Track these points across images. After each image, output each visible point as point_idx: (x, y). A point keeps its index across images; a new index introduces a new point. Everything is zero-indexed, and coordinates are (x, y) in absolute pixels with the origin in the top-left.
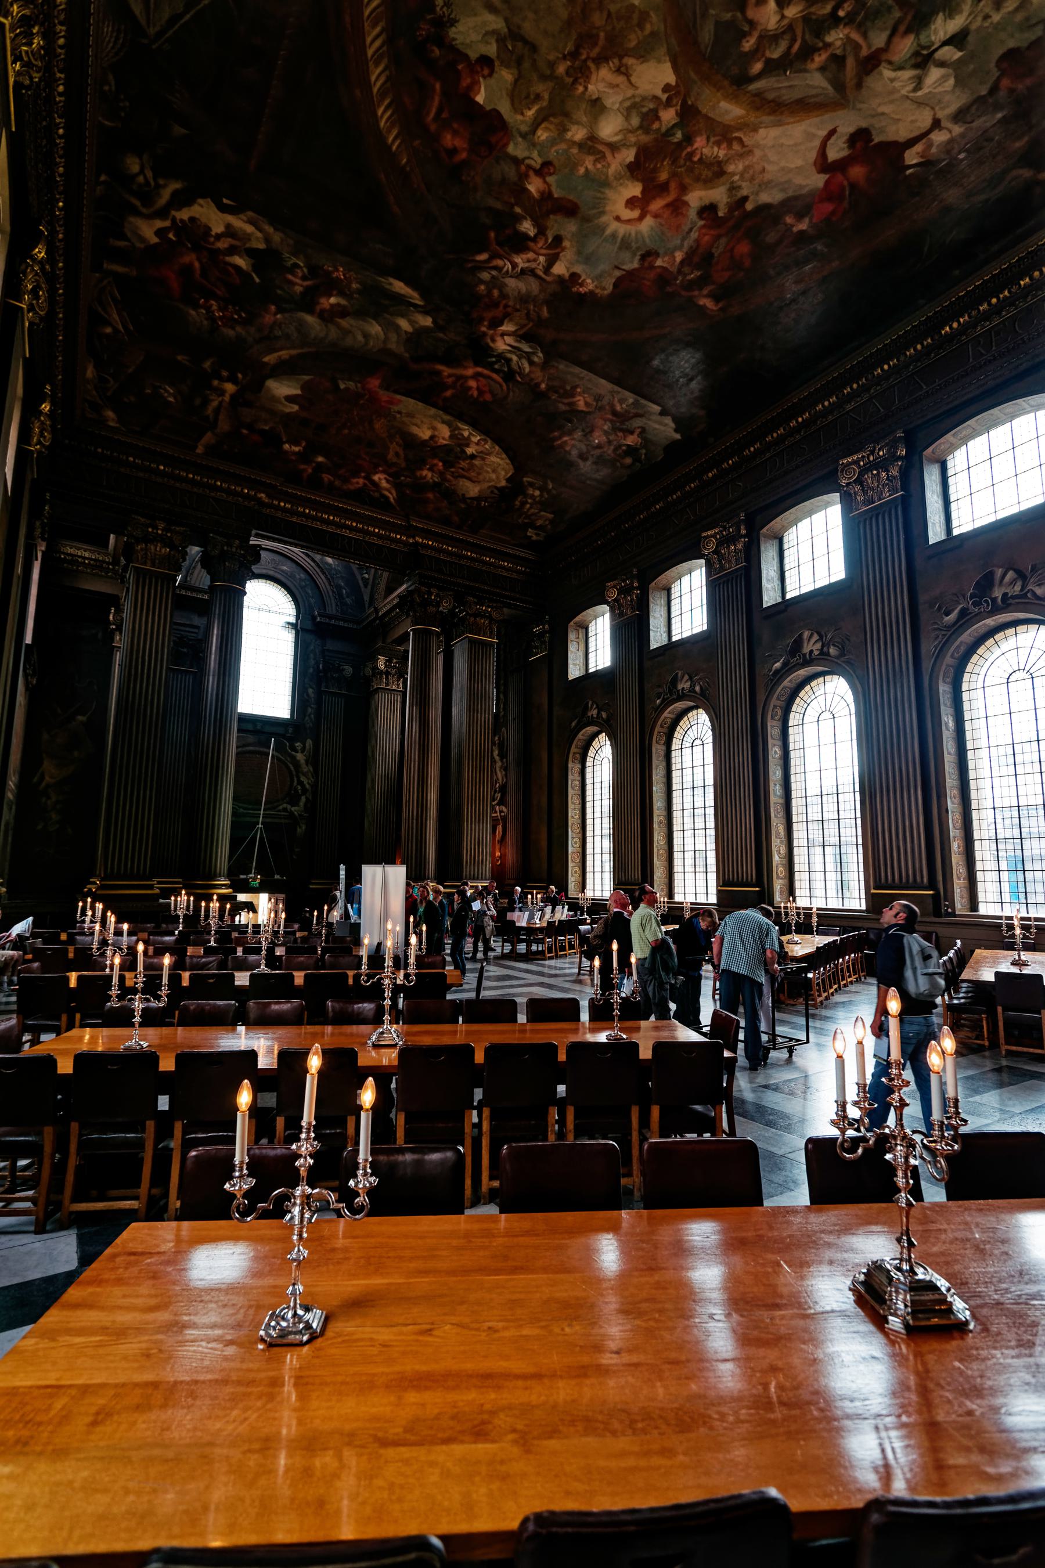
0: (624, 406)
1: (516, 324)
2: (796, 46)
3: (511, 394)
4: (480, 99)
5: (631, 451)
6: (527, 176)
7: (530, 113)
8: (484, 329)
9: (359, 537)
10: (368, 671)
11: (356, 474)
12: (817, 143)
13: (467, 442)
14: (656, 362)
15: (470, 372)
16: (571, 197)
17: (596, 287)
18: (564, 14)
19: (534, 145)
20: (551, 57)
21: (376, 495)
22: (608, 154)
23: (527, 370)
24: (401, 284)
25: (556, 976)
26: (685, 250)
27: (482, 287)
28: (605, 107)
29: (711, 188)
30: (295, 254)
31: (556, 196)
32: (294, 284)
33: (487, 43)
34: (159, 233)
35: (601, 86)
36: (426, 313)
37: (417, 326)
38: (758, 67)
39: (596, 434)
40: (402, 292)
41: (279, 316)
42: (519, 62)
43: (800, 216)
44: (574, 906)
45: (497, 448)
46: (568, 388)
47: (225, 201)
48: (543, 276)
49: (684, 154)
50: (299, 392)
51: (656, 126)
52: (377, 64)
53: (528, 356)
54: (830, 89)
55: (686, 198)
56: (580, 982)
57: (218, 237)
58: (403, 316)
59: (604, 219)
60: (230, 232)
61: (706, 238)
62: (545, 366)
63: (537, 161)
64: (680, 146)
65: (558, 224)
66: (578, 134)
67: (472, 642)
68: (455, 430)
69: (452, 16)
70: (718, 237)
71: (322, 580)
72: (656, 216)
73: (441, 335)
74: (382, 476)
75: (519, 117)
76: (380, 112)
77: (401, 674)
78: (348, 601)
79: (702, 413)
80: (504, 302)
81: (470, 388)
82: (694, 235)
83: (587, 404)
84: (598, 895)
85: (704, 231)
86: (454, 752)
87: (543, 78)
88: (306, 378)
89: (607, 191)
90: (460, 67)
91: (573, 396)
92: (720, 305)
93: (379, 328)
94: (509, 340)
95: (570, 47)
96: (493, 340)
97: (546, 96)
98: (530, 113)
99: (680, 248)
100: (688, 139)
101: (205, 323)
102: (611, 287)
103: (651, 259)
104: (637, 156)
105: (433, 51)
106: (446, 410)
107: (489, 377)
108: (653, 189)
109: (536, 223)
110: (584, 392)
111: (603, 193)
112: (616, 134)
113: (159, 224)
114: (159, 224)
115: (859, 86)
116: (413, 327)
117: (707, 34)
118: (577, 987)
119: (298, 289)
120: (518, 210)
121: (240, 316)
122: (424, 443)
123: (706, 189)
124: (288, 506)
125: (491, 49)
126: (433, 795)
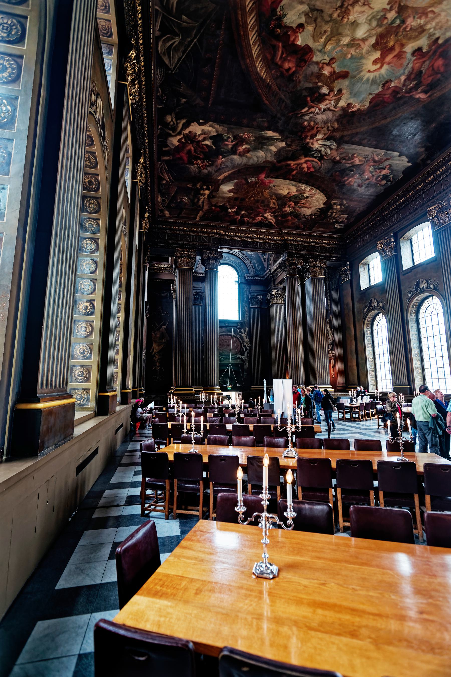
1: (323, 134)
3: (323, 165)
4: (299, 43)
5: (385, 177)
7: (322, 40)
8: (308, 141)
9: (261, 241)
10: (269, 297)
11: (257, 216)
13: (304, 192)
14: (394, 132)
15: (303, 161)
16: (346, 70)
17: (361, 106)
20: (330, 12)
21: (267, 222)
24: (271, 132)
25: (366, 429)
27: (306, 123)
28: (359, 23)
29: (418, 40)
30: (228, 133)
31: (337, 72)
32: (228, 145)
33: (301, 18)
34: (179, 141)
35: (355, 15)
36: (282, 141)
37: (278, 148)
39: (366, 174)
40: (271, 135)
41: (223, 159)
42: (315, 20)
44: (373, 396)
45: (318, 191)
46: (350, 156)
47: (201, 121)
50: (233, 187)
51: (385, 22)
52: (254, 46)
55: (404, 50)
56: (379, 432)
57: (199, 135)
59: (362, 74)
60: (204, 132)
61: (418, 65)
63: (327, 59)
64: (399, 26)
66: (346, 40)
67: (313, 279)
68: (298, 187)
69: (285, 13)
71: (247, 262)
72: (389, 63)
73: (289, 148)
74: (268, 214)
75: (318, 44)
76: (257, 65)
77: (283, 297)
78: (258, 269)
79: (423, 149)
80: (317, 126)
81: (304, 168)
82: (410, 66)
84: (385, 391)
85: (416, 62)
86: (309, 328)
87: (327, 22)
88: (235, 181)
90: (289, 33)
91: (353, 159)
93: (263, 153)
95: (339, 4)
96: (313, 144)
97: (329, 30)
98: (322, 40)
100: (403, 22)
101: (197, 170)
102: (368, 104)
103: (387, 85)
104: (377, 40)
105: (278, 31)
106: (293, 180)
107: (312, 161)
108: (386, 51)
110: (358, 156)
111: (360, 62)
113: (179, 137)
114: (179, 137)
118: (378, 435)
119: (230, 147)
120: (320, 84)
121: (209, 164)
122: (285, 196)
123: (415, 42)
124: (232, 234)
125: (303, 20)
126: (301, 348)
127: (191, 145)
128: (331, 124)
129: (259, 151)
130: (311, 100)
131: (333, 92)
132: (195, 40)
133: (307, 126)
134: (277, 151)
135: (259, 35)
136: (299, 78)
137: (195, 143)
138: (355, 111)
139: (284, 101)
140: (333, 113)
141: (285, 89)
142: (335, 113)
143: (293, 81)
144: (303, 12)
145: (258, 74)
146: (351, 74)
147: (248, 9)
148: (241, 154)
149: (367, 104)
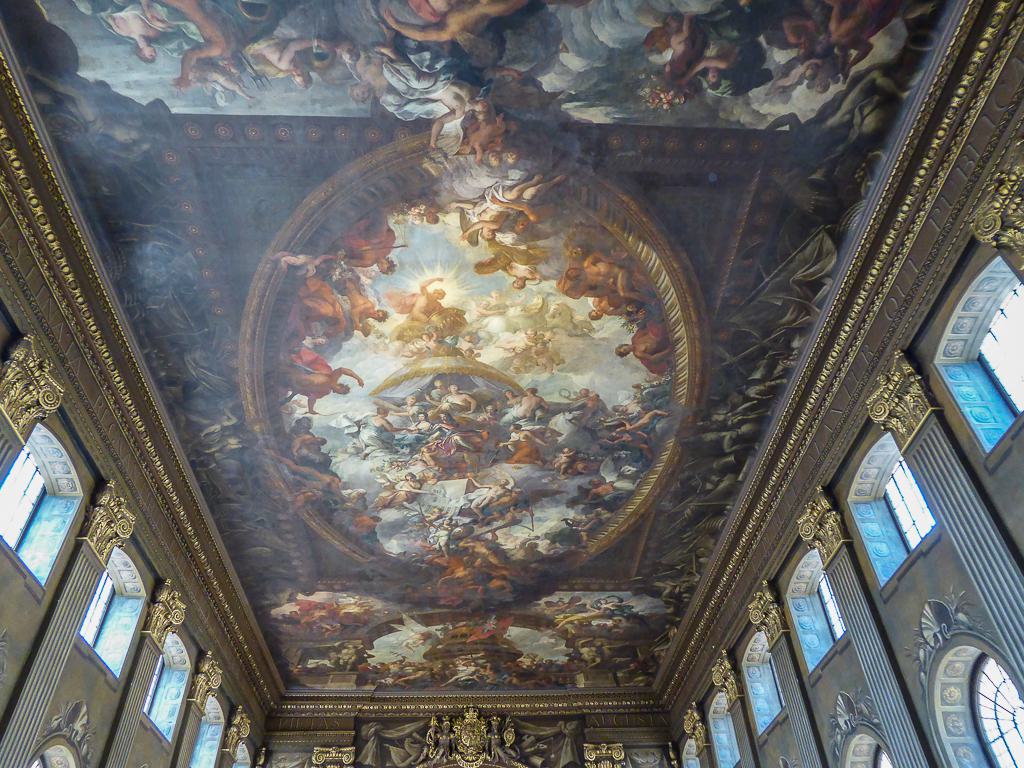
0: (218, 88)
2: (428, 398)
3: (373, 13)
4: (590, 300)
6: (531, 273)
7: (552, 308)
8: (478, 108)
12: (362, 377)
15: (455, 23)
16: (487, 275)
18: (562, 355)
19: (539, 293)
20: (557, 337)
22: (481, 310)
23: (387, 74)
29: (396, 328)
30: (718, 101)
31: (500, 271)
32: (719, 57)
34: (866, 49)
35: (518, 339)
36: (554, 95)
37: (557, 68)
38: (438, 384)
40: (593, 111)
43: (316, 346)
46: (313, 75)
48: (462, 205)
49: (435, 336)
51: (467, 338)
52: (667, 286)
53: (405, 98)
54: (388, 396)
55: (405, 316)
57: (799, 83)
58: (581, 76)
59: (451, 274)
61: (361, 301)
64: (443, 338)
65: (484, 252)
70: (353, 306)
72: (414, 295)
73: (523, 68)
80: (479, 156)
82: (372, 299)
83: (268, 62)
85: (369, 305)
89: (465, 292)
92: (283, 264)
93: (601, 38)
94: (440, 109)
95: (550, 345)
96: (458, 97)
100: (440, 341)
103: (386, 266)
107: (424, 28)
108: (433, 307)
109: (499, 244)
110: (289, 79)
112: (488, 323)
113: (863, 65)
114: (863, 65)
115: (375, 403)
116: (562, 64)
117: (479, 381)
119: (711, 52)
125: (595, 324)
127: (834, 38)
128: (445, 168)
129: (617, 46)
131: (487, 237)
132: (767, 280)
133: (502, 152)
134: (557, 52)
135: (660, 302)
136: (571, 252)
137: (819, 49)
139: (588, 205)
140: (457, 195)
141: (593, 231)
142: (454, 197)
144: (598, 331)
145: (654, 246)
146: (472, 268)
147: (682, 323)
148: (674, 25)
149: (398, 230)
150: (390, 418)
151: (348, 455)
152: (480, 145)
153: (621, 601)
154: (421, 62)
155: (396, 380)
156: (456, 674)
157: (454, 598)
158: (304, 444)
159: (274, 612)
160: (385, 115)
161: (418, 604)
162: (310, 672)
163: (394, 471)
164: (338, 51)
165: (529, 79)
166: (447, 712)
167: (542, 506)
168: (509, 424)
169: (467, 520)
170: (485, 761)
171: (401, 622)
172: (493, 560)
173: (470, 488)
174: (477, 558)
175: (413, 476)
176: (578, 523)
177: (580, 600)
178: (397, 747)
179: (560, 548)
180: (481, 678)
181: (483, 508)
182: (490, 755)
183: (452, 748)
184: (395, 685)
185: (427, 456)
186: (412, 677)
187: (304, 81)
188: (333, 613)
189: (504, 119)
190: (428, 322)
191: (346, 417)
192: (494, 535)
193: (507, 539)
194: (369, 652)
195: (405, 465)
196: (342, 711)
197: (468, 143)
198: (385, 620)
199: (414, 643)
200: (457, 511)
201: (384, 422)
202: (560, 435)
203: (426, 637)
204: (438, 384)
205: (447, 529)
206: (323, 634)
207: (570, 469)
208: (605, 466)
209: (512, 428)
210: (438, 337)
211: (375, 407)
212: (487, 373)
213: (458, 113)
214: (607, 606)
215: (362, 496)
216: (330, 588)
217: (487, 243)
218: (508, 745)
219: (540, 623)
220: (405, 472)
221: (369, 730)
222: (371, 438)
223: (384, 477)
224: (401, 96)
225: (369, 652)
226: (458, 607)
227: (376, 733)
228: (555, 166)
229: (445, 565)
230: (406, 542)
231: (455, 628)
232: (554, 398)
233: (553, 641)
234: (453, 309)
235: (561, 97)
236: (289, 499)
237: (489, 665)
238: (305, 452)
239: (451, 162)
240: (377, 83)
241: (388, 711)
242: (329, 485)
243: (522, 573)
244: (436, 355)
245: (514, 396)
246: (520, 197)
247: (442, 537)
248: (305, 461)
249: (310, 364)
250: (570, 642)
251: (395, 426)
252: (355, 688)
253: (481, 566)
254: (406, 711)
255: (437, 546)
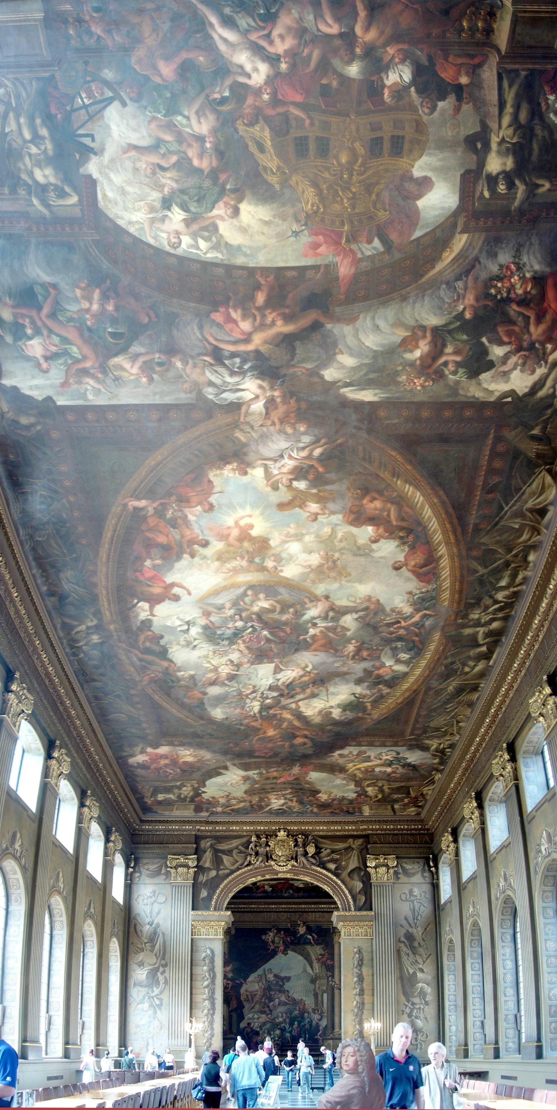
1: (253, 414)
2: (242, 603)
3: (199, 335)
6: (322, 509)
7: (340, 535)
8: (276, 393)
12: (191, 589)
16: (286, 513)
17: (222, 474)
19: (328, 524)
23: (208, 374)
26: (192, 522)
36: (334, 383)
37: (335, 365)
38: (249, 592)
46: (155, 376)
51: (272, 558)
53: (221, 389)
58: (353, 369)
59: (258, 512)
62: (197, 388)
64: (253, 558)
65: (284, 495)
72: (229, 528)
73: (309, 366)
82: (197, 531)
87: (341, 549)
93: (367, 344)
94: (248, 396)
96: (261, 387)
99: (196, 522)
100: (251, 561)
103: (207, 507)
104: (269, 544)
109: (296, 489)
115: (201, 608)
116: (339, 362)
117: (282, 590)
120: (314, 491)
130: (316, 468)
133: (296, 423)
134: (335, 354)
138: (225, 465)
139: (364, 459)
140: (262, 455)
143: (359, 489)
150: (212, 619)
151: (179, 647)
152: (279, 419)
153: (398, 754)
154: (233, 365)
155: (216, 590)
156: (267, 806)
157: (266, 751)
158: (147, 638)
159: (131, 761)
160: (207, 400)
161: (239, 755)
162: (160, 803)
163: (216, 658)
164: (173, 360)
165: (315, 373)
166: (264, 832)
167: (336, 684)
168: (307, 622)
169: (275, 694)
170: (293, 866)
171: (226, 768)
172: (296, 723)
173: (277, 670)
174: (284, 722)
175: (232, 662)
176: (364, 696)
177: (365, 752)
178: (227, 855)
179: (350, 715)
180: (289, 808)
181: (288, 685)
182: (297, 861)
183: (268, 857)
184: (223, 813)
185: (242, 647)
186: (236, 807)
187: (148, 380)
188: (175, 762)
189: (298, 400)
190: (241, 547)
191: (178, 618)
192: (299, 707)
193: (307, 708)
194: (203, 789)
195: (226, 653)
196: (185, 830)
197: (269, 418)
198: (214, 766)
199: (237, 783)
200: (268, 687)
201: (207, 622)
202: (348, 630)
203: (246, 779)
204: (249, 592)
205: (259, 701)
206: (167, 776)
207: (357, 656)
208: (386, 654)
209: (310, 625)
210: (249, 558)
211: (201, 611)
212: (289, 584)
213: (261, 398)
214: (388, 757)
215: (192, 677)
216: (171, 744)
217: (286, 489)
218: (310, 855)
219: (334, 769)
220: (224, 660)
221: (205, 844)
222: (198, 633)
223: (209, 662)
224: (218, 388)
225: (203, 789)
226: (270, 757)
227: (212, 846)
228: (337, 432)
229: (259, 727)
230: (228, 710)
231: (268, 772)
232: (343, 602)
233: (345, 782)
234: (260, 537)
235: (340, 384)
236: (137, 679)
237: (295, 799)
238: (148, 644)
239: (256, 431)
240: (201, 380)
241: (219, 831)
242: (167, 668)
243: (320, 734)
244: (247, 570)
245: (312, 601)
246: (309, 457)
247: (256, 706)
248: (148, 651)
249: (151, 579)
250: (358, 783)
251: (217, 625)
252: (194, 814)
253: (287, 728)
254: (232, 831)
255: (252, 713)
